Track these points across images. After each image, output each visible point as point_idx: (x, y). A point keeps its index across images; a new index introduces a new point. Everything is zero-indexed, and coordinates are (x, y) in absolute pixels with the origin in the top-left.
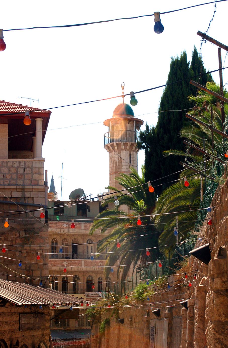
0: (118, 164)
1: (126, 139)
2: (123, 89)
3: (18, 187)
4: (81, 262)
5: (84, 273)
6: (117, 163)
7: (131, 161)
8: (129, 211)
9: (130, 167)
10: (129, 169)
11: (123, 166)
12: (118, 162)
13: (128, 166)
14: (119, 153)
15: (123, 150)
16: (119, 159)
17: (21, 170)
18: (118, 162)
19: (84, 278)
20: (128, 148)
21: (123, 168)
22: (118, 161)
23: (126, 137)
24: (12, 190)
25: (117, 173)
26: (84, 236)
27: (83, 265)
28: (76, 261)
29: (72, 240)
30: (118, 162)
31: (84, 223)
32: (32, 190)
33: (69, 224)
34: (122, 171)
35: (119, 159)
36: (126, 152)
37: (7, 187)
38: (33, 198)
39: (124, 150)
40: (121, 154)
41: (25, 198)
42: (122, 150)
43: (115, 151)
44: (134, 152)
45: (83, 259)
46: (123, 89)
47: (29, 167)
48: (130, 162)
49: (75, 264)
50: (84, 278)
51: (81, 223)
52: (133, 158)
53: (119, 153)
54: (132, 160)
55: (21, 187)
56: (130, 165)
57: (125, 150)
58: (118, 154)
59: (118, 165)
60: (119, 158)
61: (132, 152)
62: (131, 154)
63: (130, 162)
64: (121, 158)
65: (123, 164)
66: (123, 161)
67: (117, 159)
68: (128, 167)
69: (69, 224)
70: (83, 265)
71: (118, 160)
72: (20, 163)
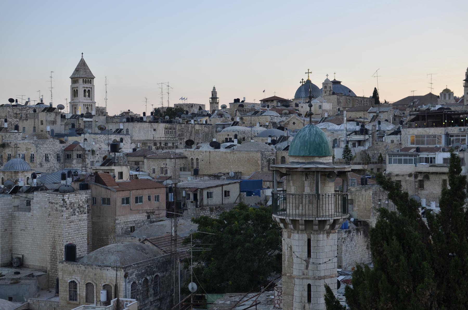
1: (300, 208)
9: (307, 267)
10: (306, 271)
11: (294, 265)
13: (303, 265)
21: (294, 267)
25: (286, 275)
34: (292, 273)
36: (299, 237)
40: (292, 238)
52: (315, 248)
54: (314, 252)
56: (308, 263)
58: (288, 237)
61: (314, 234)
62: (312, 239)
65: (295, 260)
71: (288, 249)
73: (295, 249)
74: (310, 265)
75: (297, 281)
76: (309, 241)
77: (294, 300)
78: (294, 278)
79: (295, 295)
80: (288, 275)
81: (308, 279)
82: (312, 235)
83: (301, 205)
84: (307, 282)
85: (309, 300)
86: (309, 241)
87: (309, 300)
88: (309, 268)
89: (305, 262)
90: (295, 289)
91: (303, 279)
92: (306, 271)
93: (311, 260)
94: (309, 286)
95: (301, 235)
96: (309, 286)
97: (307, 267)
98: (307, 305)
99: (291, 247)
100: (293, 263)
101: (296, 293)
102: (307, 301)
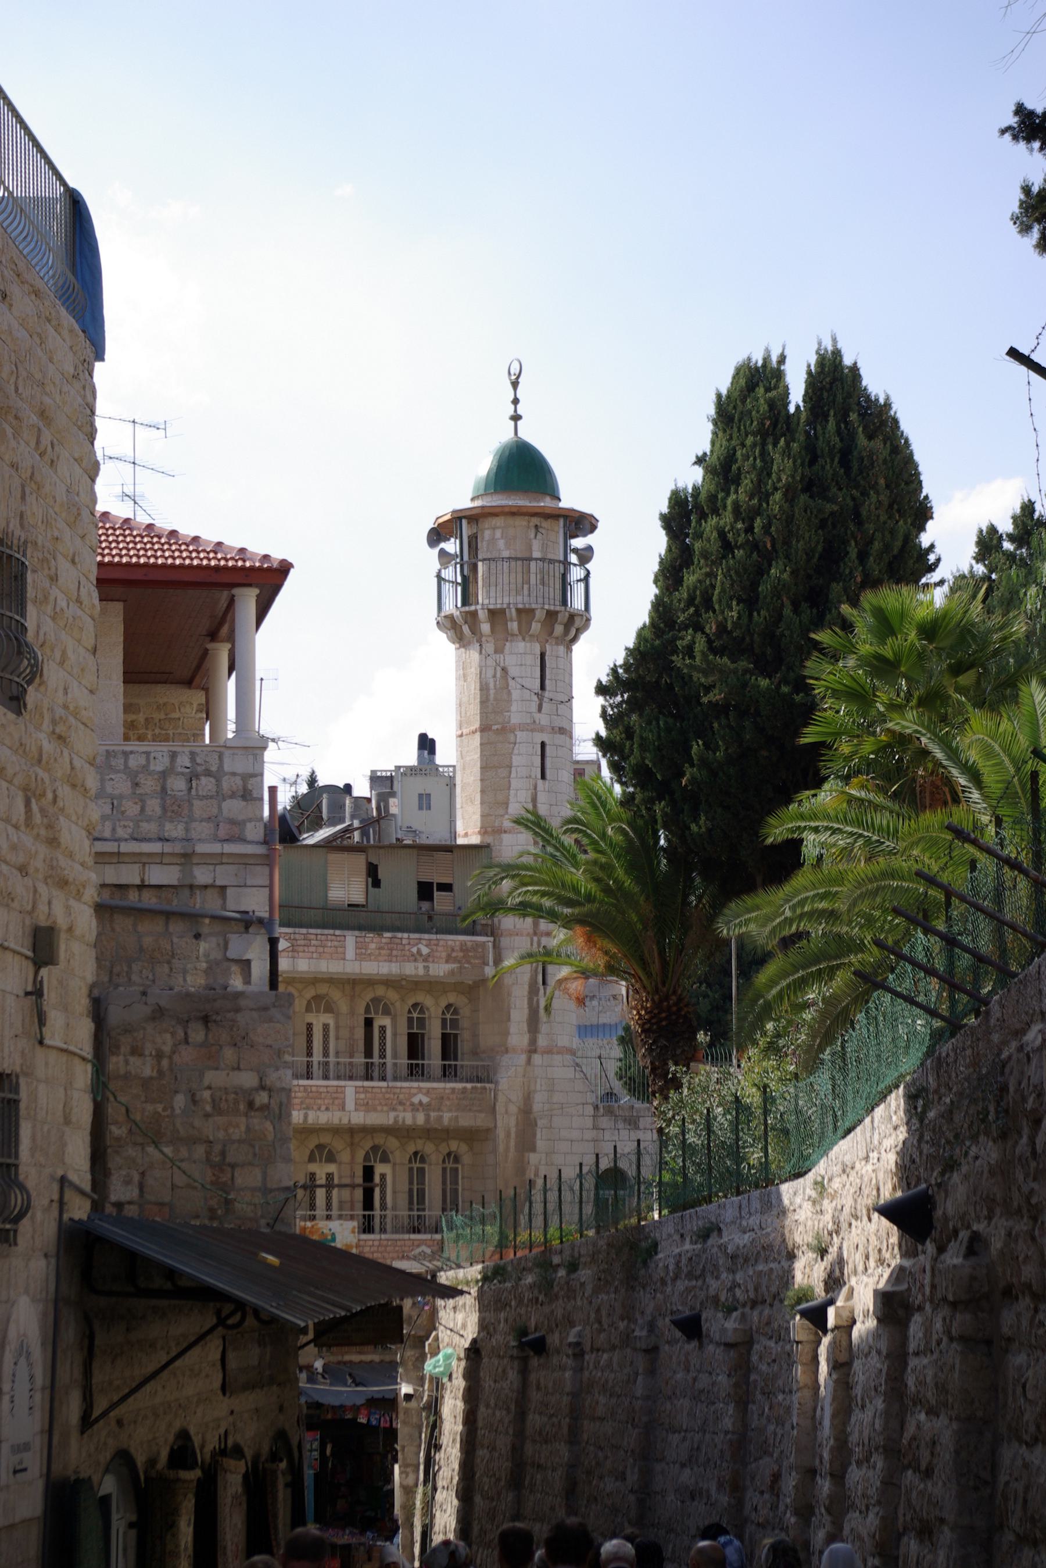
0: (492, 692)
1: (526, 592)
2: (515, 384)
3: (168, 848)
4: (340, 1090)
5: (352, 1137)
6: (488, 689)
7: (547, 682)
9: (540, 709)
10: (537, 716)
11: (514, 704)
14: (499, 650)
15: (513, 635)
16: (498, 675)
17: (177, 785)
18: (492, 686)
19: (353, 1157)
20: (536, 627)
21: (514, 708)
22: (495, 682)
23: (526, 587)
24: (143, 860)
26: (353, 988)
27: (350, 1105)
28: (322, 1090)
29: (305, 1002)
30: (495, 685)
31: (357, 933)
32: (218, 860)
33: (297, 936)
35: (498, 675)
36: (526, 647)
37: (125, 847)
38: (223, 888)
39: (520, 638)
41: (191, 887)
42: (509, 636)
43: (484, 639)
44: (557, 644)
45: (351, 1078)
46: (515, 384)
47: (208, 773)
48: (543, 687)
49: (319, 1101)
50: (353, 1157)
51: (346, 933)
53: (499, 650)
55: (178, 848)
56: (541, 698)
57: (524, 639)
58: (496, 652)
59: (495, 699)
60: (499, 669)
61: (551, 644)
63: (543, 687)
64: (504, 669)
65: (516, 694)
66: (511, 683)
67: (490, 673)
68: (534, 707)
69: (297, 936)
70: (350, 1105)
71: (494, 676)
72: (173, 756)
73: (513, 671)
74: (544, 705)
75: (520, 736)
76: (543, 656)
77: (513, 775)
78: (513, 731)
79: (514, 764)
80: (495, 727)
81: (542, 730)
82: (548, 647)
83: (526, 587)
84: (539, 738)
85: (543, 777)
86: (543, 656)
87: (543, 777)
88: (544, 710)
89: (535, 698)
90: (516, 751)
91: (532, 731)
92: (537, 716)
93: (547, 694)
94: (543, 745)
95: (528, 645)
96: (543, 745)
97: (540, 709)
98: (540, 782)
99: (504, 669)
100: (509, 701)
101: (516, 760)
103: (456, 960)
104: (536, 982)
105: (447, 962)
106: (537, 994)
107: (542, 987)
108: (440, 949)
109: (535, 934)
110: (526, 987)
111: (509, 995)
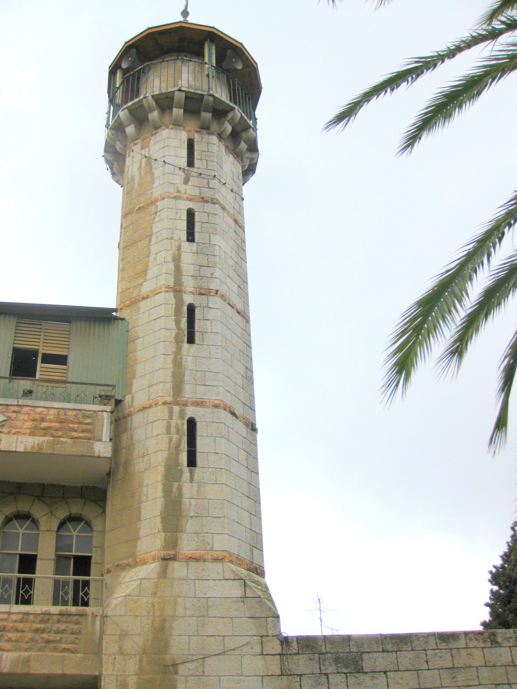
8: (179, 349)
10: (183, 188)
12: (136, 181)
22: (140, 173)
48: (191, 163)
54: (201, 160)
63: (191, 163)
84: (184, 206)
85: (191, 237)
87: (191, 237)
92: (183, 188)
94: (191, 215)
98: (186, 246)
102: (184, 235)
103: (46, 431)
104: (177, 464)
105: (32, 434)
106: (179, 478)
107: (186, 470)
108: (22, 417)
109: (177, 403)
110: (161, 469)
111: (141, 485)
